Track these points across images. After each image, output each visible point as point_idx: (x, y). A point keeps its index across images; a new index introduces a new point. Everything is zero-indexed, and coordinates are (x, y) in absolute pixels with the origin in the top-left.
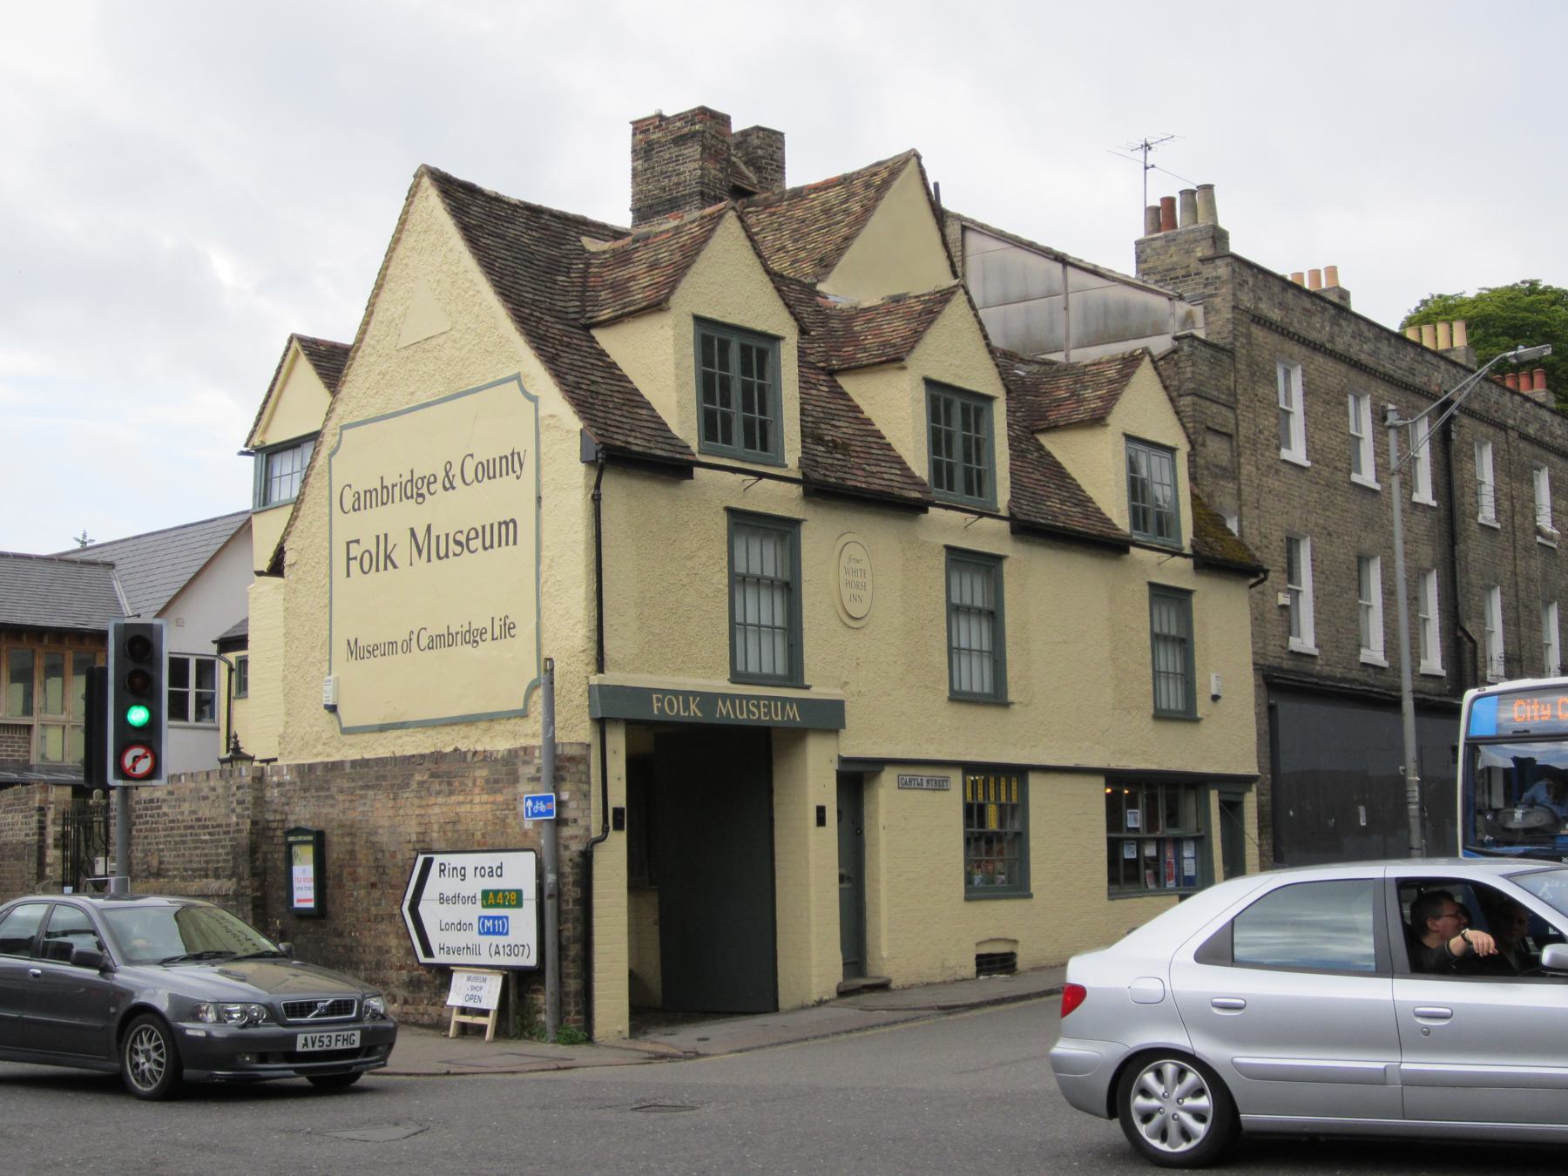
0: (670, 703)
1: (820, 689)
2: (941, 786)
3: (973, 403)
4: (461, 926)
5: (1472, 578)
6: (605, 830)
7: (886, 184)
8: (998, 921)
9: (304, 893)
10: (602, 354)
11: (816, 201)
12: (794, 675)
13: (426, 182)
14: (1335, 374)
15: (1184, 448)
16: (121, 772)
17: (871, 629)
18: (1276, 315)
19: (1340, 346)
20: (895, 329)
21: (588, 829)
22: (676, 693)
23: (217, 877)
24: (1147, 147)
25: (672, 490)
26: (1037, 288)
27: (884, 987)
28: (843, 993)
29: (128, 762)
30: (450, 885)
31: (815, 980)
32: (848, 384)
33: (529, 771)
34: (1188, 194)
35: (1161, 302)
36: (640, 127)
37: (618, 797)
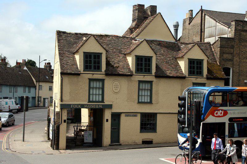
0: (75, 106)
1: (106, 103)
2: (136, 116)
6: (61, 123)
8: (148, 136)
12: (103, 101)
21: (59, 122)
22: (76, 105)
25: (78, 77)
26: (213, 25)
27: (120, 145)
28: (110, 145)
31: (105, 143)
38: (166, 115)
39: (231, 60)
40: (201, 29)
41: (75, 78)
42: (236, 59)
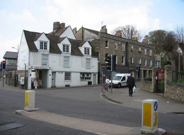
2: (62, 73)
7: (67, 28)
14: (113, 41)
15: (91, 48)
17: (55, 62)
18: (106, 37)
19: (114, 39)
26: (89, 34)
28: (51, 87)
32: (58, 44)
34: (104, 26)
38: (75, 73)
39: (99, 49)
40: (83, 36)
41: (35, 54)
42: (101, 49)
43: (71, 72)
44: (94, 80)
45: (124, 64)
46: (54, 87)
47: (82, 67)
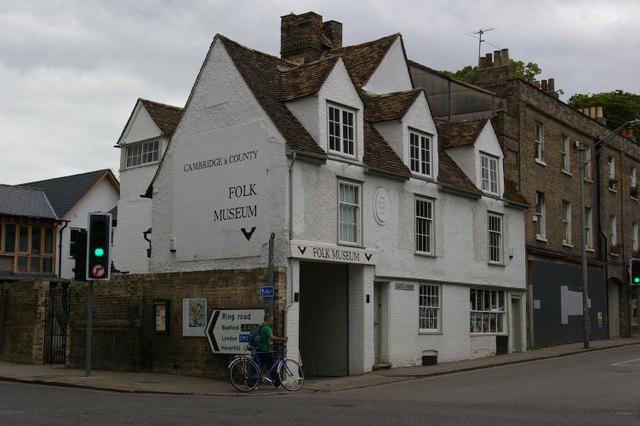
2: (411, 288)
3: (426, 137)
4: (231, 339)
5: (606, 212)
7: (387, 48)
9: (161, 326)
10: (290, 113)
11: (358, 52)
13: (218, 41)
14: (556, 129)
15: (502, 157)
16: (91, 275)
18: (535, 103)
20: (397, 106)
23: (120, 318)
24: (481, 32)
29: (95, 271)
30: (228, 323)
33: (261, 277)
35: (490, 98)
36: (284, 19)
37: (297, 289)
43: (442, 283)
44: (514, 322)
45: (590, 246)
46: (382, 366)
47: (477, 259)
